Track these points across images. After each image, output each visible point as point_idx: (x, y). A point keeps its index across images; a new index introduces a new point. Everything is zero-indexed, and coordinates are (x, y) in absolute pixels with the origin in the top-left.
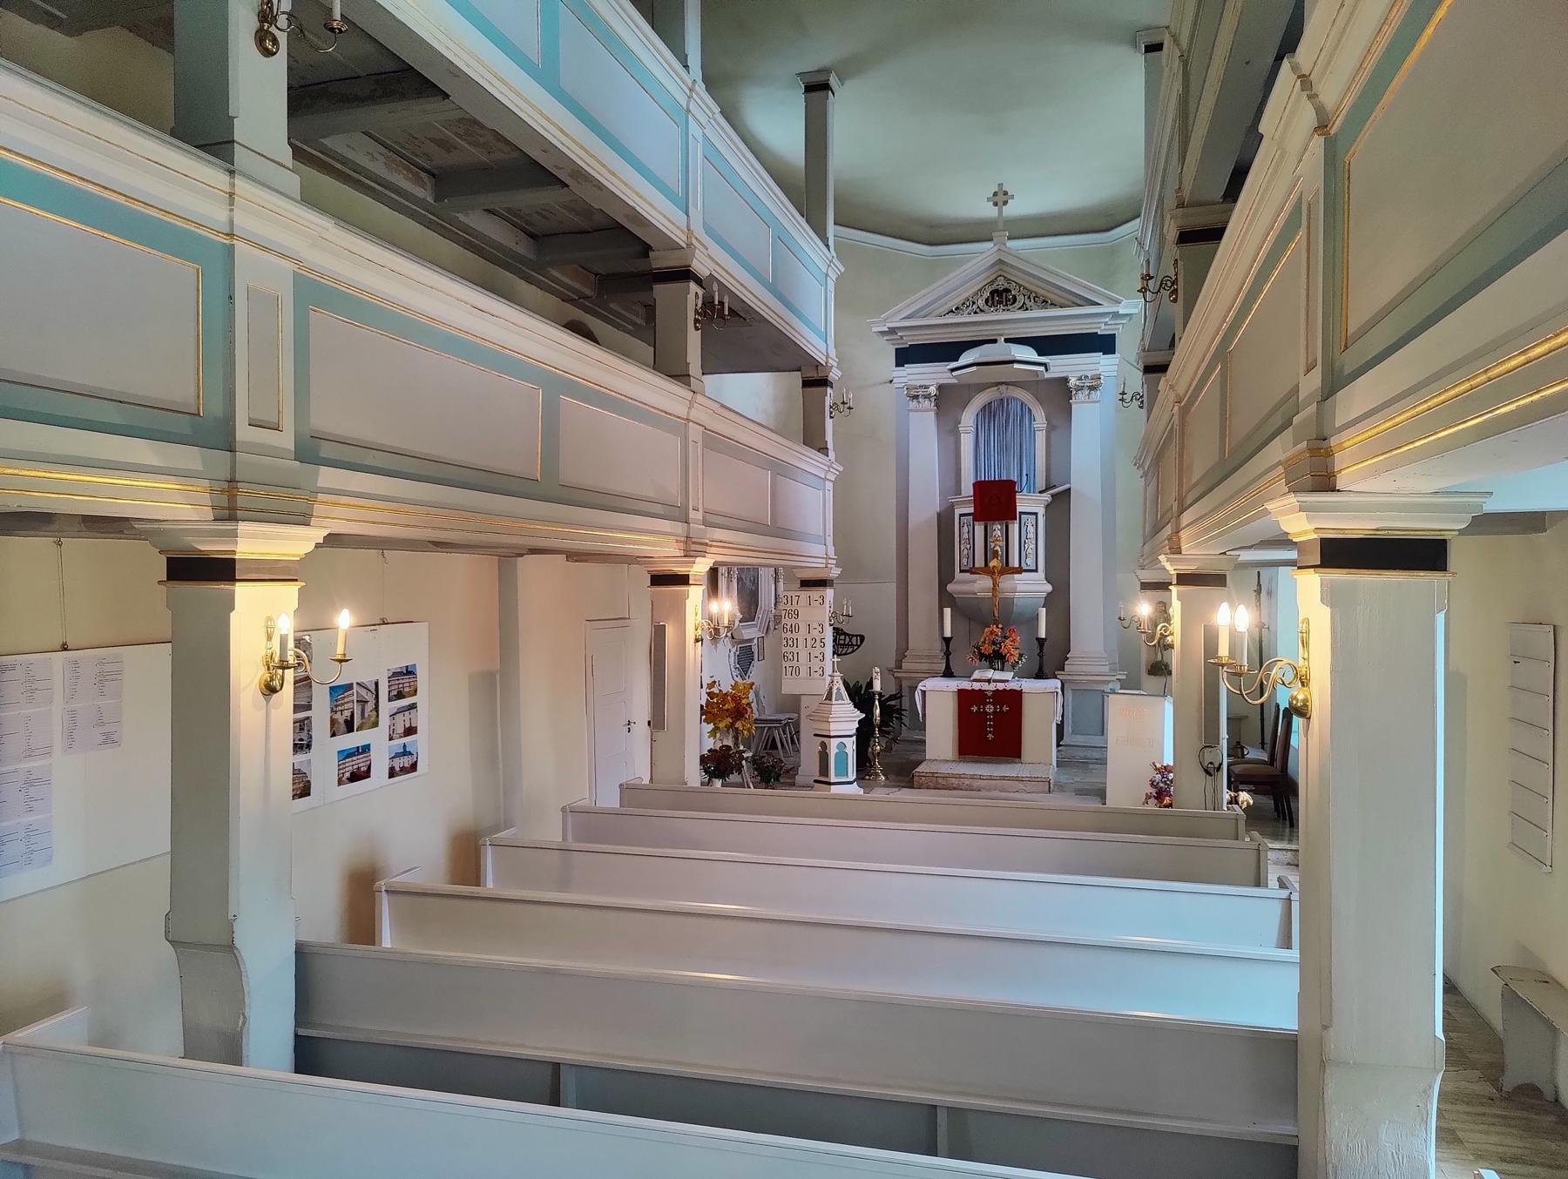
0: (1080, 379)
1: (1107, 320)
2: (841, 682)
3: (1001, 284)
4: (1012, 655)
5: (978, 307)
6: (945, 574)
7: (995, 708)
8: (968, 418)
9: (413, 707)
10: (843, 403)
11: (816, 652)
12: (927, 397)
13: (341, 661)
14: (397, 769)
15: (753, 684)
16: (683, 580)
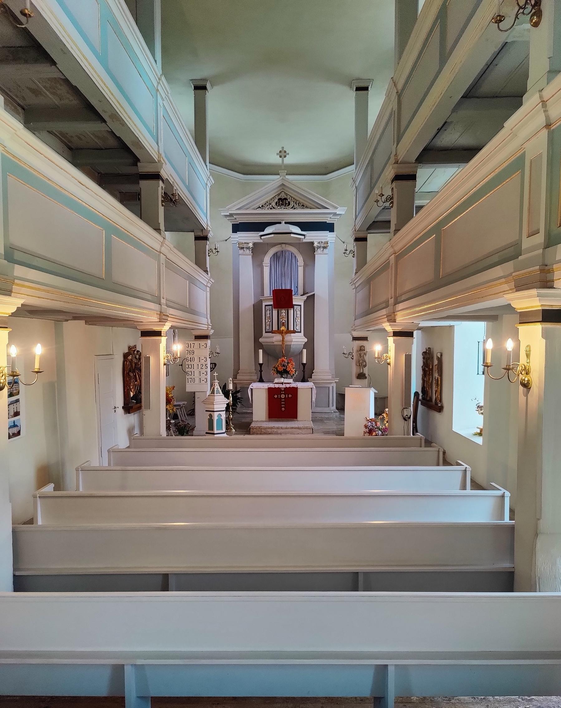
0: (319, 243)
1: (331, 216)
3: (283, 196)
4: (292, 371)
5: (272, 206)
6: (258, 334)
7: (286, 396)
8: (267, 260)
9: (17, 401)
11: (203, 371)
12: (248, 248)
13: (37, 372)
14: (11, 434)
15: (174, 387)
16: (158, 334)
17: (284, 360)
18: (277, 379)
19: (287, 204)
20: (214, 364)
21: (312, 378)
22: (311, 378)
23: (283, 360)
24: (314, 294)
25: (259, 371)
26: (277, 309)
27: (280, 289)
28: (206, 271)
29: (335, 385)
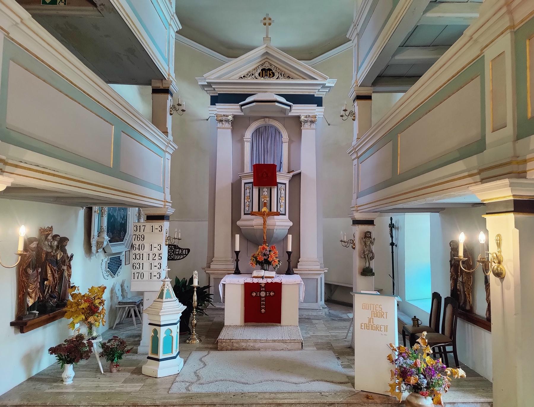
2: (170, 285)
4: (275, 261)
6: (236, 215)
7: (266, 294)
8: (248, 134)
10: (179, 105)
11: (156, 263)
17: (265, 248)
18: (256, 272)
20: (187, 250)
23: (264, 247)
26: (257, 187)
27: (262, 163)
28: (166, 133)
29: (323, 276)
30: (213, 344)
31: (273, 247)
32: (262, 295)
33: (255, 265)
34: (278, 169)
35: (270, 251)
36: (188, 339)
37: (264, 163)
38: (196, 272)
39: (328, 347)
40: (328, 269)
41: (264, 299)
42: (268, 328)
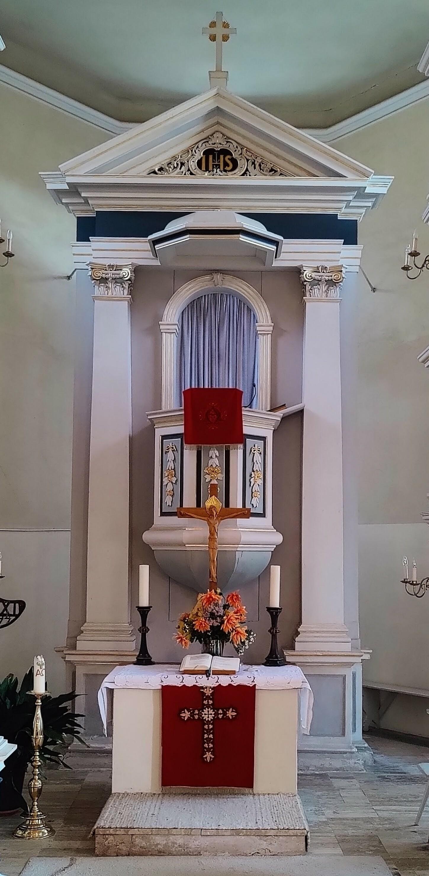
1: (351, 198)
3: (218, 143)
4: (238, 633)
5: (189, 170)
7: (216, 714)
12: (119, 281)
17: (214, 600)
18: (191, 658)
19: (228, 166)
20: (17, 605)
21: (296, 650)
22: (293, 648)
23: (211, 597)
24: (301, 412)
25: (139, 630)
26: (195, 446)
27: (206, 387)
30: (84, 838)
31: (233, 595)
32: (206, 717)
33: (188, 641)
34: (245, 401)
35: (226, 607)
36: (19, 827)
37: (211, 386)
38: (41, 659)
39: (371, 848)
40: (371, 651)
41: (211, 726)
42: (221, 800)
